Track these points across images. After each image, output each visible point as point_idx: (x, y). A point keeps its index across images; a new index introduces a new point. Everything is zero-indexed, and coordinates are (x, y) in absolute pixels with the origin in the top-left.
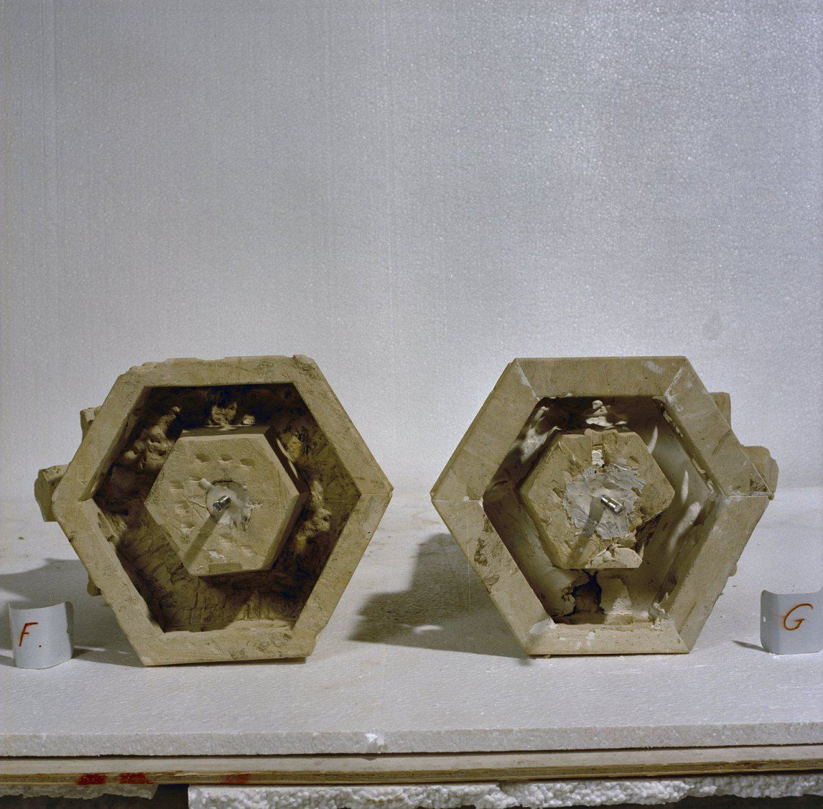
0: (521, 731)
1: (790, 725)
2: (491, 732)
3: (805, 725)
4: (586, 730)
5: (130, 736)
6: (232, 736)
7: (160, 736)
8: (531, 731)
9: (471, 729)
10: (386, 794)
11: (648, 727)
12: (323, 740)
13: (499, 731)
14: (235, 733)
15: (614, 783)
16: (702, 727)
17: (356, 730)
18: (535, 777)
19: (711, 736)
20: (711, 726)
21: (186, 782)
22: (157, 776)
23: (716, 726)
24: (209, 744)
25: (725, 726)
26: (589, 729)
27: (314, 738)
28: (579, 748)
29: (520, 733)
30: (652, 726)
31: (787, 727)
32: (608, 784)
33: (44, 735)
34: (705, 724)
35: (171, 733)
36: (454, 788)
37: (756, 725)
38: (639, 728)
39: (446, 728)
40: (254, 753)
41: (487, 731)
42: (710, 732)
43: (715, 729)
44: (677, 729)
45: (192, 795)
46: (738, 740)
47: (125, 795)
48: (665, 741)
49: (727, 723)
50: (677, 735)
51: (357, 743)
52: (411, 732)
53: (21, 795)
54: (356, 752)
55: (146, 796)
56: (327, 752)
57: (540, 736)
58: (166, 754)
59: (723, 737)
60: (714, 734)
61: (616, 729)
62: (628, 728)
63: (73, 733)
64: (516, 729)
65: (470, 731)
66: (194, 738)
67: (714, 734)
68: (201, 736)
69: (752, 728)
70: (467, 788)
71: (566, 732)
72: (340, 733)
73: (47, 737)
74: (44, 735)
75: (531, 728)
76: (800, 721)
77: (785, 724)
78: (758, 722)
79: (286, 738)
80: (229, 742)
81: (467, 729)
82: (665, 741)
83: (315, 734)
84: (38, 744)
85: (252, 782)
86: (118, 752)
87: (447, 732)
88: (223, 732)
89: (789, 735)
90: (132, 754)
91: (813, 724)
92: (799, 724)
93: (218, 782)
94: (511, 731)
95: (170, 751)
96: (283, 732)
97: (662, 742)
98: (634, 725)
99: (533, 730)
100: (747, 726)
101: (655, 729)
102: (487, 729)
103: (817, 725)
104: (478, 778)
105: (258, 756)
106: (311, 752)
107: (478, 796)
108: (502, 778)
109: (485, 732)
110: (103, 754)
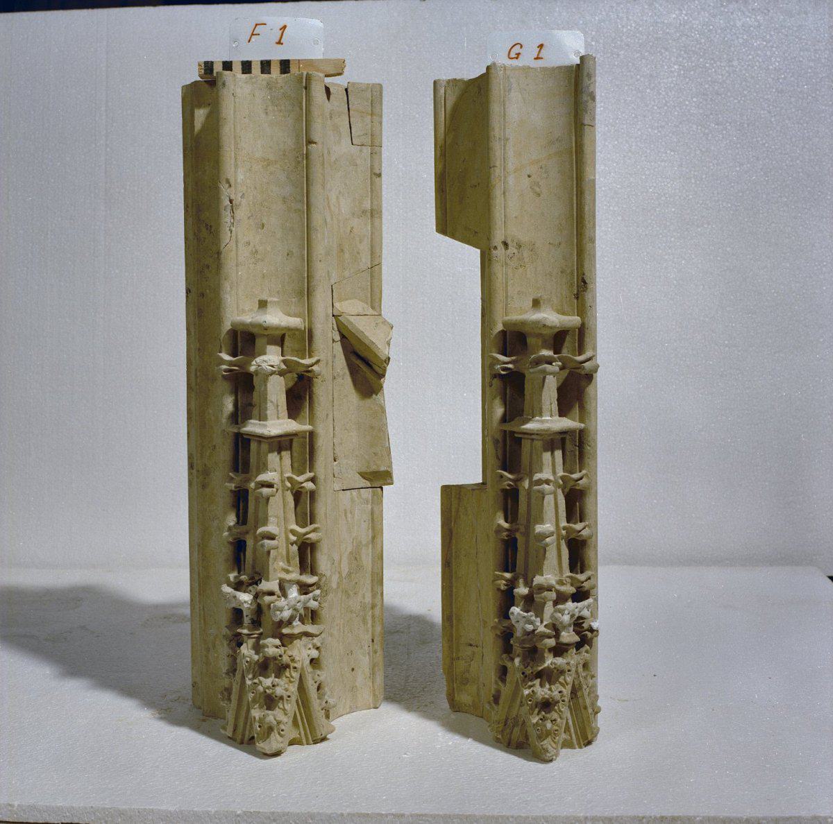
1: (643, 818)
2: (387, 815)
5: (86, 808)
6: (170, 812)
8: (420, 815)
11: (520, 816)
12: (245, 818)
13: (393, 814)
14: (172, 809)
20: (574, 817)
26: (470, 815)
27: (238, 816)
29: (411, 816)
33: (16, 803)
35: (119, 807)
37: (613, 817)
38: (512, 817)
41: (383, 815)
49: (588, 815)
52: (319, 813)
63: (39, 803)
66: (139, 812)
72: (259, 812)
73: (19, 805)
74: (16, 803)
75: (419, 813)
77: (638, 817)
78: (615, 815)
80: (167, 816)
81: (366, 812)
83: (238, 812)
84: (10, 811)
87: (349, 814)
88: (163, 807)
91: (662, 817)
92: (651, 817)
96: (212, 810)
98: (508, 814)
99: (422, 815)
102: (383, 813)
103: (666, 818)
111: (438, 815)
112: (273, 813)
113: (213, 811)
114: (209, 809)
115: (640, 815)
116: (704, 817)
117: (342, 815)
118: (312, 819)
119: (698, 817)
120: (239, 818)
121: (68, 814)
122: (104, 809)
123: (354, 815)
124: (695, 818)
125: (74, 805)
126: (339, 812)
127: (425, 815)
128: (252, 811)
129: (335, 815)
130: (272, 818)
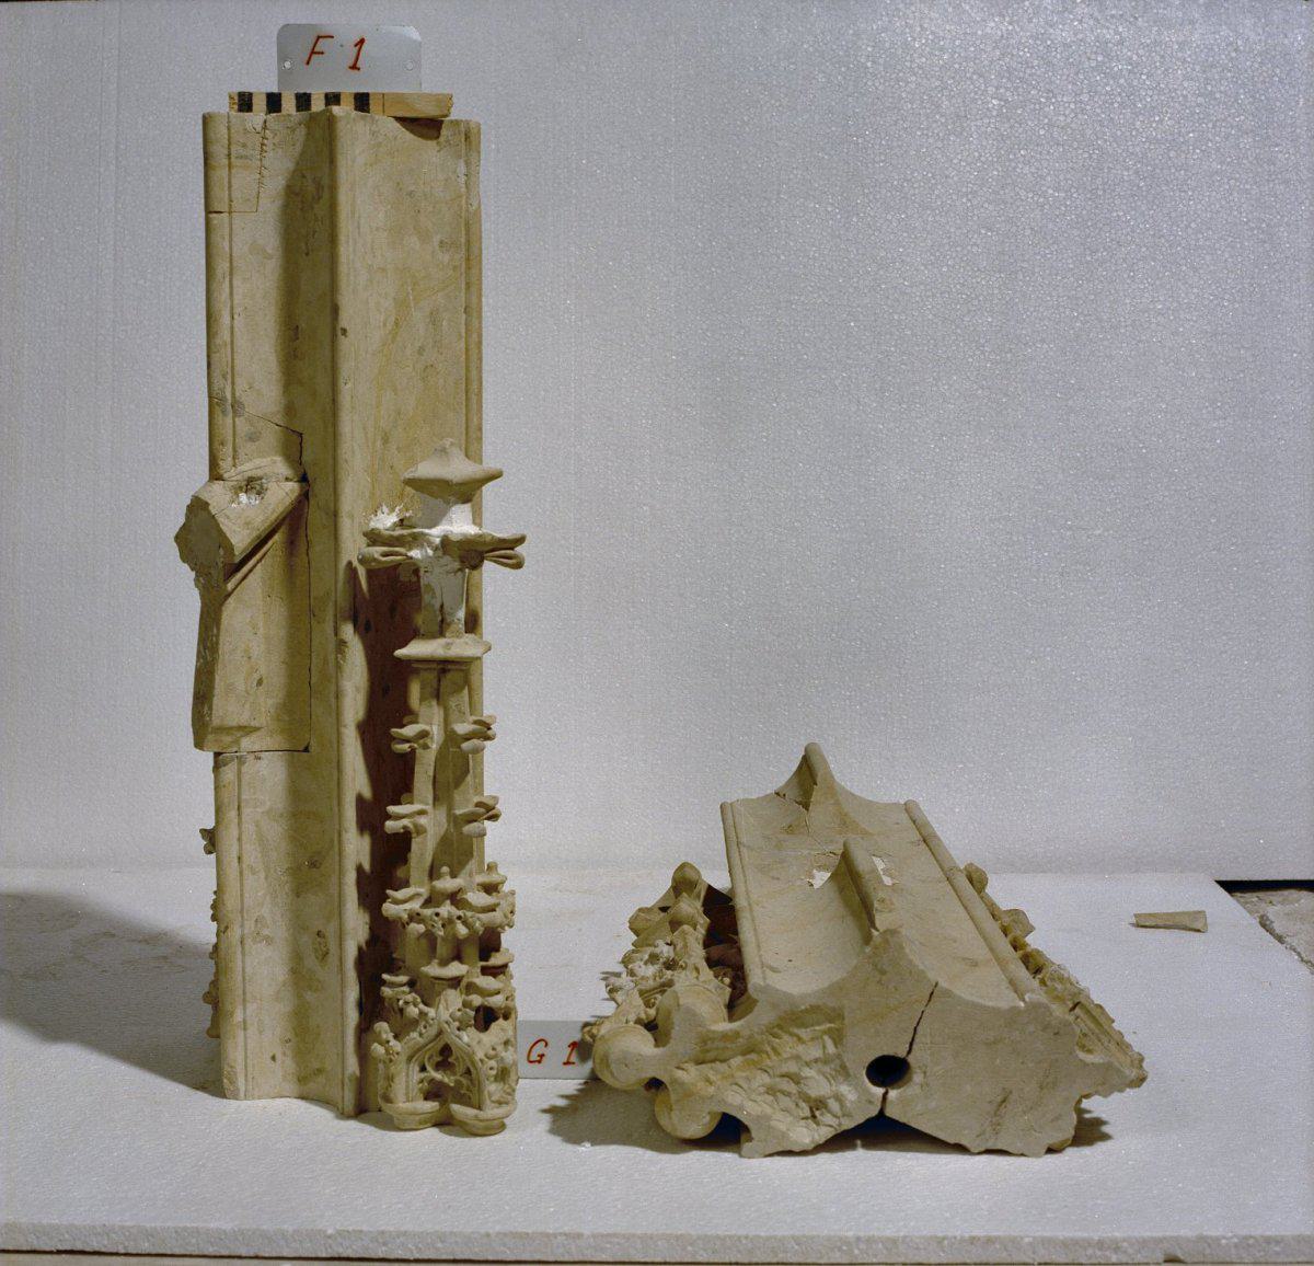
0: (594, 1236)
1: (944, 1238)
2: (555, 1235)
3: (963, 1240)
4: (678, 1238)
6: (225, 1231)
7: (132, 1227)
8: (608, 1235)
9: (530, 1231)
11: (759, 1237)
13: (565, 1235)
14: (228, 1226)
16: (829, 1239)
17: (383, 1228)
19: (840, 1249)
20: (840, 1239)
23: (846, 1237)
24: (194, 1241)
25: (858, 1239)
26: (681, 1235)
27: (329, 1237)
28: (668, 1260)
30: (762, 1234)
31: (940, 1241)
34: (832, 1233)
39: (498, 1228)
40: (252, 1254)
42: (839, 1244)
43: (848, 1243)
44: (797, 1240)
46: (876, 1256)
48: (781, 1255)
49: (862, 1234)
50: (796, 1247)
51: (385, 1244)
52: (451, 1233)
54: (381, 1256)
56: (345, 1255)
57: (618, 1244)
58: (140, 1252)
59: (856, 1252)
60: (844, 1248)
61: (718, 1237)
62: (730, 1237)
64: (587, 1232)
65: (528, 1234)
67: (844, 1248)
68: (185, 1229)
69: (894, 1241)
71: (651, 1238)
72: (361, 1231)
76: (958, 1234)
77: (937, 1237)
78: (902, 1234)
79: (292, 1236)
82: (781, 1255)
83: (330, 1232)
86: (79, 1247)
87: (498, 1234)
89: (944, 1251)
90: (97, 1249)
91: (974, 1238)
92: (955, 1238)
94: (580, 1236)
95: (146, 1247)
96: (288, 1227)
97: (777, 1256)
98: (742, 1232)
100: (888, 1239)
101: (768, 1239)
105: (257, 1257)
106: (324, 1255)
109: (547, 1235)
110: (61, 1248)
111: (634, 1235)
112: (383, 1232)
113: (291, 1229)
114: (286, 1226)
115: (940, 1235)
116: (1034, 1238)
117: (488, 1235)
118: (442, 1242)
119: (1028, 1237)
120: (330, 1241)
121: (67, 1236)
122: (123, 1227)
123: (505, 1235)
124: (1022, 1238)
125: (76, 1222)
126: (483, 1231)
127: (615, 1235)
128: (350, 1229)
129: (476, 1235)
130: (381, 1240)
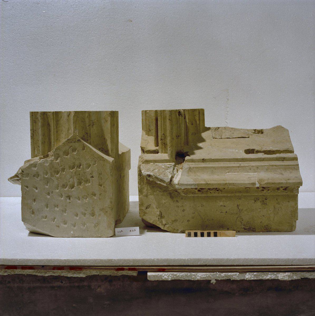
10: (205, 275)
15: (271, 273)
18: (248, 271)
21: (147, 270)
22: (139, 269)
32: (270, 273)
36: (227, 273)
45: (149, 274)
47: (129, 275)
53: (99, 275)
55: (135, 275)
70: (229, 274)
85: (166, 271)
93: (156, 271)
104: (232, 271)
107: (232, 276)
108: (240, 271)
